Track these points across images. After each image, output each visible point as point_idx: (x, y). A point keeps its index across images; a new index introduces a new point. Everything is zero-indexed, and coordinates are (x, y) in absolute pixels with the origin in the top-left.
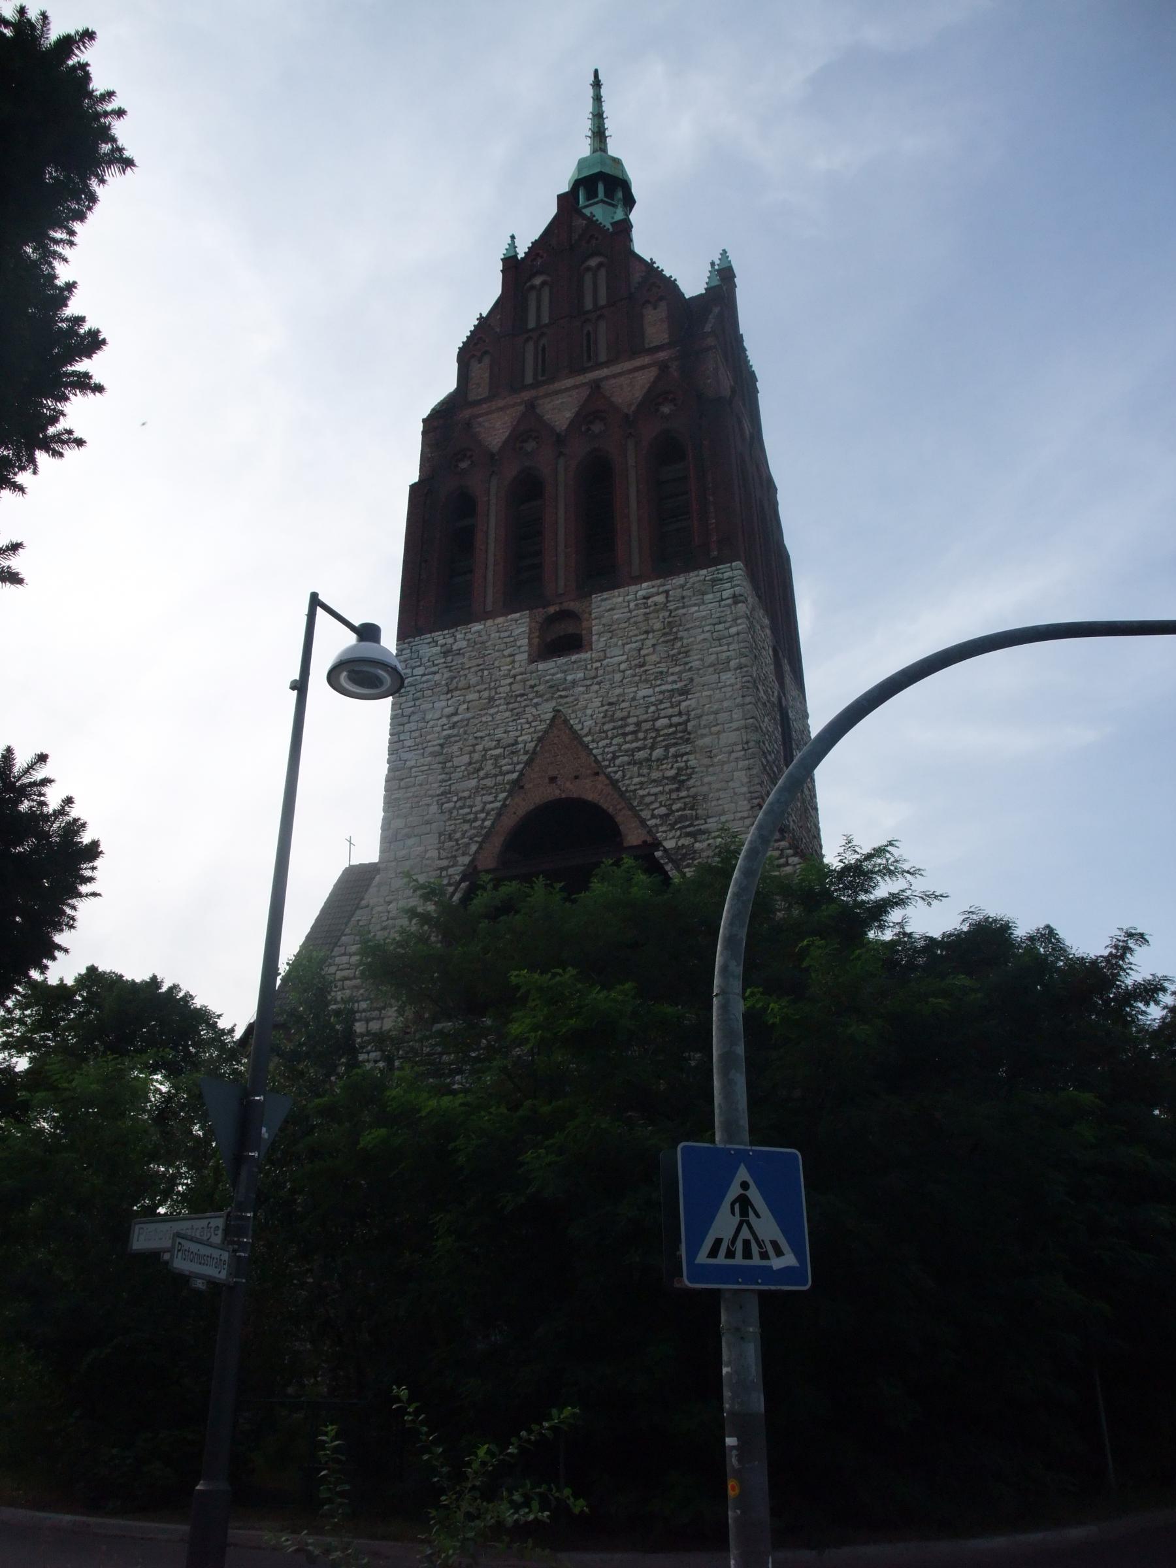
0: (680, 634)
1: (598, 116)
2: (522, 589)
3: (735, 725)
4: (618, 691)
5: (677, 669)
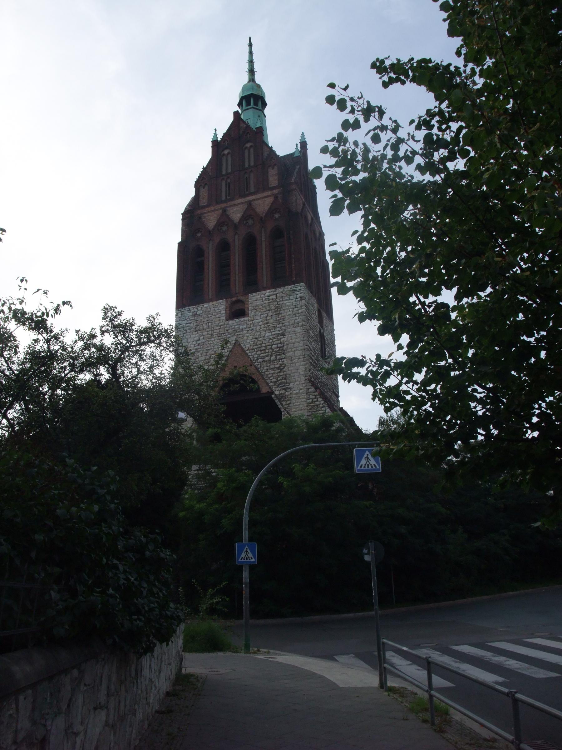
0: (281, 312)
1: (251, 62)
2: (223, 289)
3: (300, 348)
4: (258, 333)
5: (280, 325)
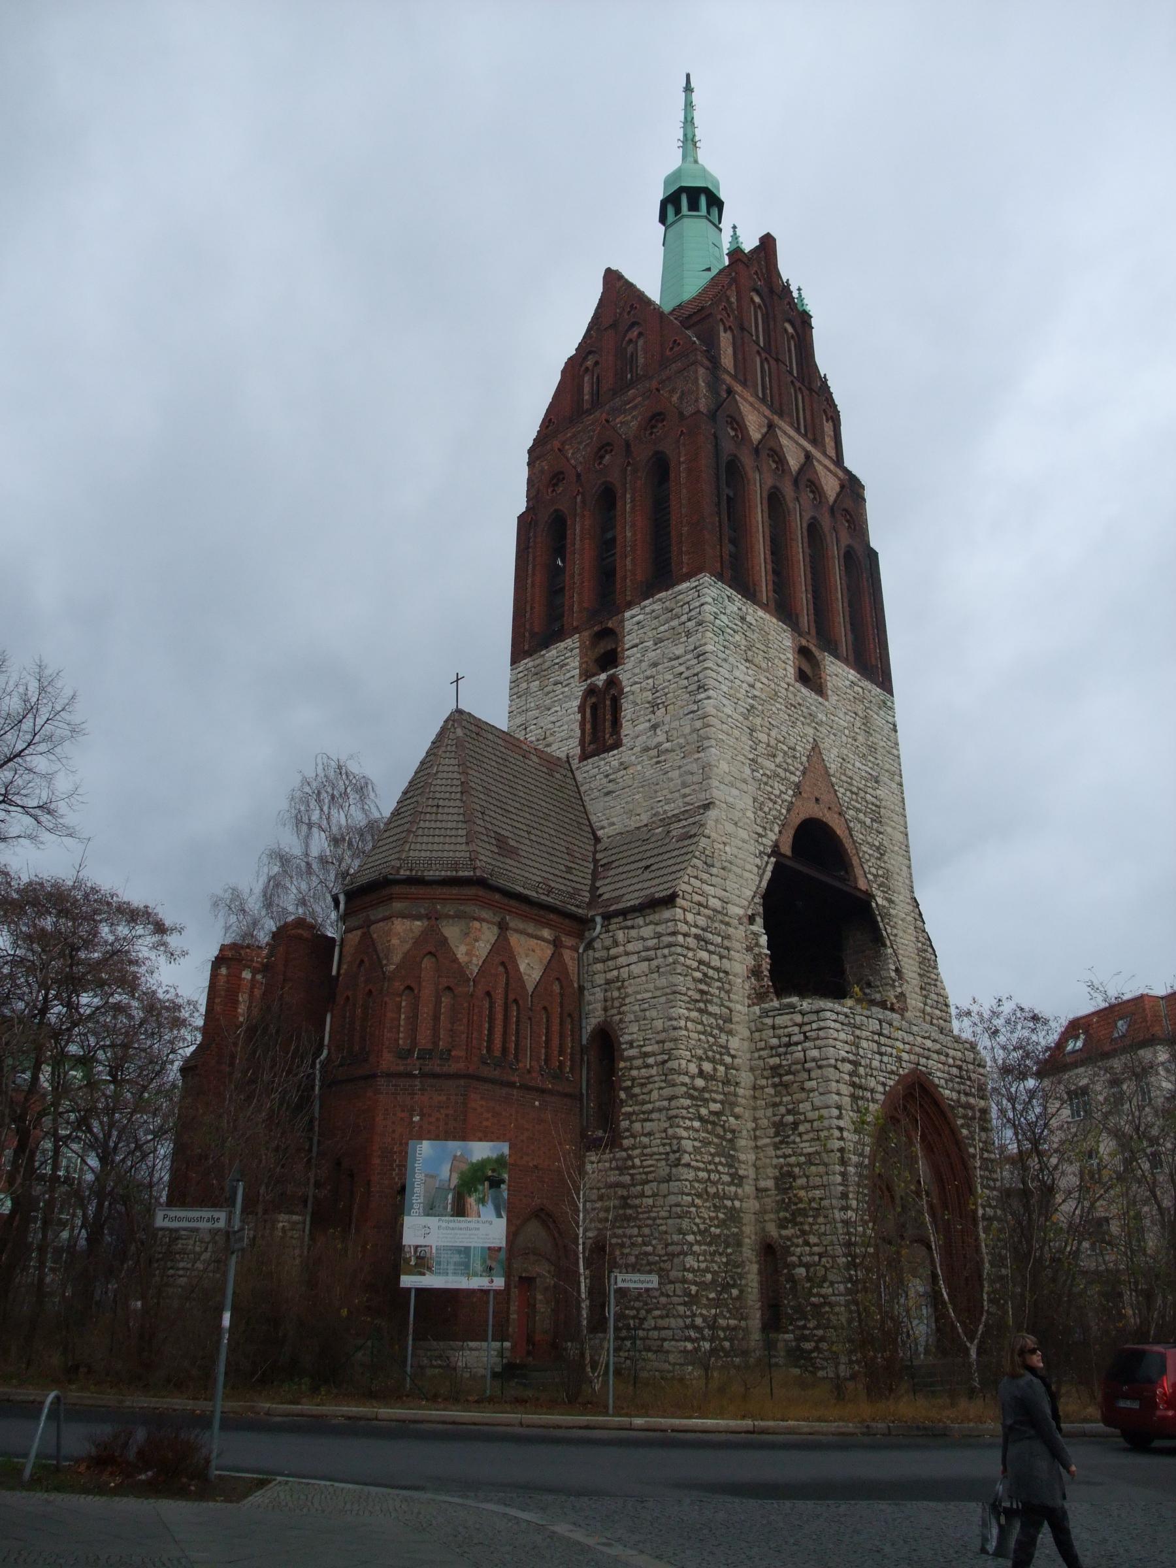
1: (689, 122)
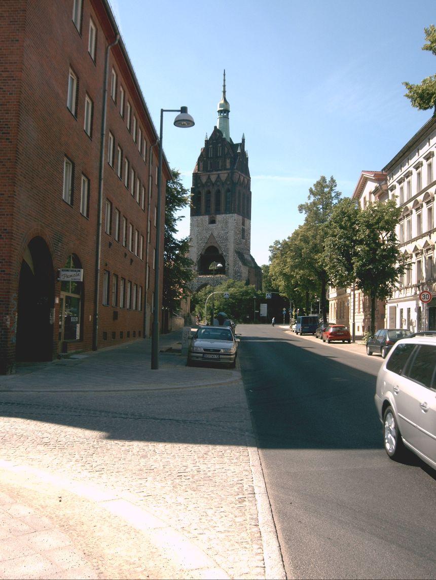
2: (207, 212)
